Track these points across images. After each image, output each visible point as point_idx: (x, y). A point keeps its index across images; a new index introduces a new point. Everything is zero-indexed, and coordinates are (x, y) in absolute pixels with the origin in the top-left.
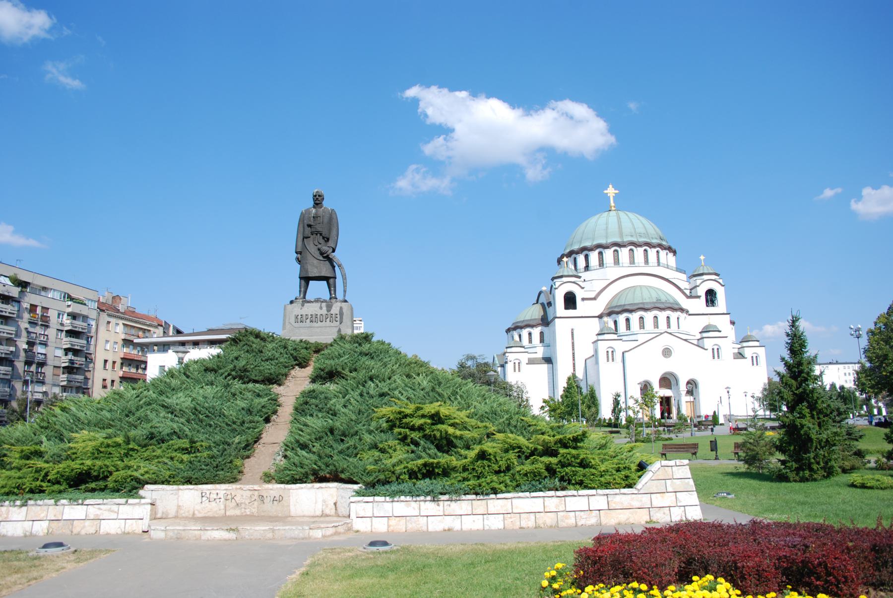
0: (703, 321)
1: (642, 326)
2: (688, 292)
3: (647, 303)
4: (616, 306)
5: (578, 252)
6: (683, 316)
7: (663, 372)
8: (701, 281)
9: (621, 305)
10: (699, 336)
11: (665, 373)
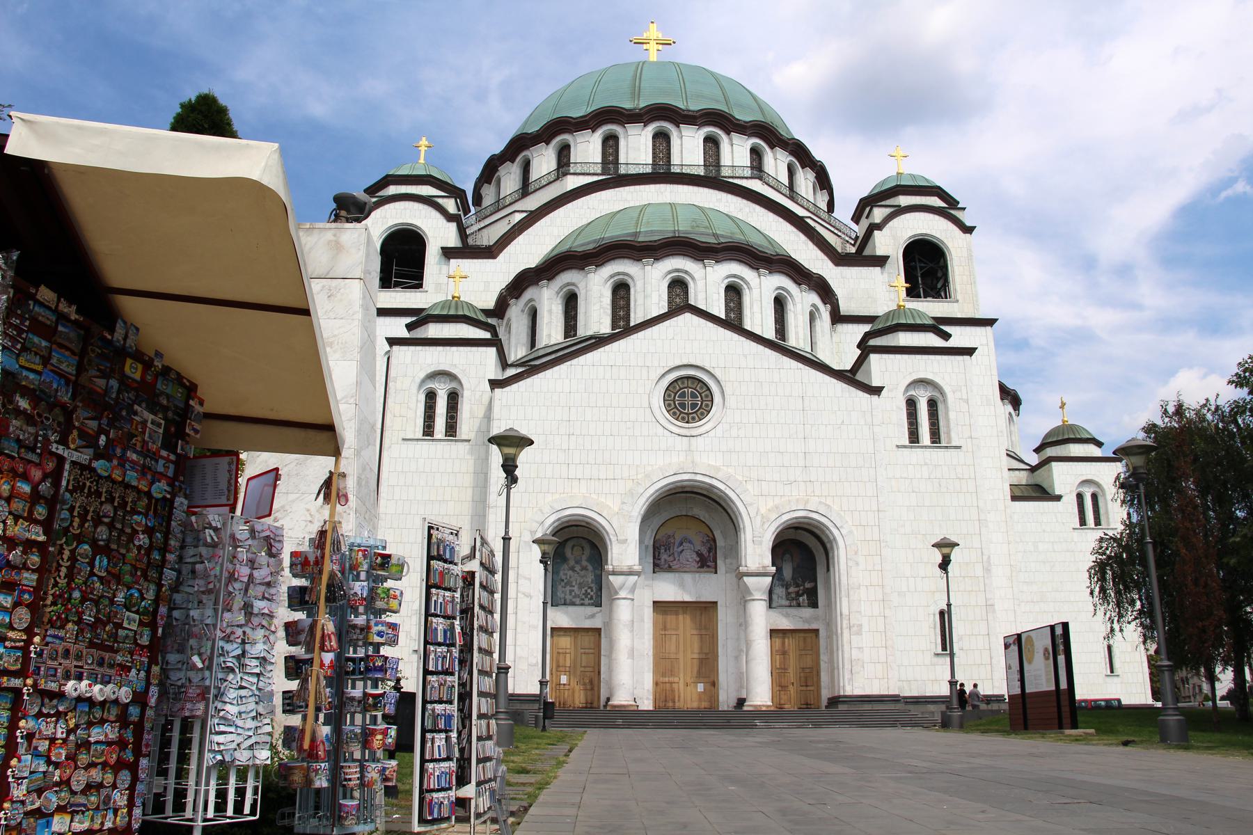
6: (802, 301)
8: (888, 211)
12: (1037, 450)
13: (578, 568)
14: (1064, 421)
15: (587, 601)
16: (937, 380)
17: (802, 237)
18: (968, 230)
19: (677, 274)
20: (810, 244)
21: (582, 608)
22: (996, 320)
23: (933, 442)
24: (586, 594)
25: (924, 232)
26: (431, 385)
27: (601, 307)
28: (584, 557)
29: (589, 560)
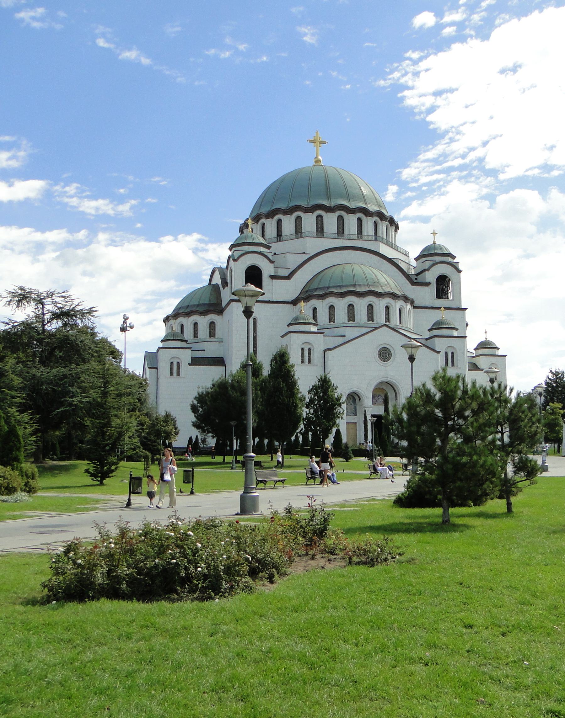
0: (435, 316)
1: (351, 316)
2: (413, 278)
3: (360, 285)
4: (317, 289)
5: (271, 215)
7: (378, 381)
9: (324, 288)
10: (427, 335)
11: (381, 383)
12: (475, 349)
13: (349, 404)
14: (486, 339)
15: (352, 414)
16: (455, 347)
17: (401, 274)
18: (460, 272)
19: (370, 303)
20: (403, 276)
21: (351, 416)
22: (467, 309)
23: (452, 366)
24: (352, 412)
25: (444, 272)
26: (303, 346)
27: (345, 313)
28: (351, 401)
29: (353, 402)
